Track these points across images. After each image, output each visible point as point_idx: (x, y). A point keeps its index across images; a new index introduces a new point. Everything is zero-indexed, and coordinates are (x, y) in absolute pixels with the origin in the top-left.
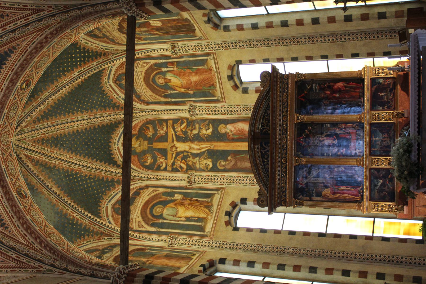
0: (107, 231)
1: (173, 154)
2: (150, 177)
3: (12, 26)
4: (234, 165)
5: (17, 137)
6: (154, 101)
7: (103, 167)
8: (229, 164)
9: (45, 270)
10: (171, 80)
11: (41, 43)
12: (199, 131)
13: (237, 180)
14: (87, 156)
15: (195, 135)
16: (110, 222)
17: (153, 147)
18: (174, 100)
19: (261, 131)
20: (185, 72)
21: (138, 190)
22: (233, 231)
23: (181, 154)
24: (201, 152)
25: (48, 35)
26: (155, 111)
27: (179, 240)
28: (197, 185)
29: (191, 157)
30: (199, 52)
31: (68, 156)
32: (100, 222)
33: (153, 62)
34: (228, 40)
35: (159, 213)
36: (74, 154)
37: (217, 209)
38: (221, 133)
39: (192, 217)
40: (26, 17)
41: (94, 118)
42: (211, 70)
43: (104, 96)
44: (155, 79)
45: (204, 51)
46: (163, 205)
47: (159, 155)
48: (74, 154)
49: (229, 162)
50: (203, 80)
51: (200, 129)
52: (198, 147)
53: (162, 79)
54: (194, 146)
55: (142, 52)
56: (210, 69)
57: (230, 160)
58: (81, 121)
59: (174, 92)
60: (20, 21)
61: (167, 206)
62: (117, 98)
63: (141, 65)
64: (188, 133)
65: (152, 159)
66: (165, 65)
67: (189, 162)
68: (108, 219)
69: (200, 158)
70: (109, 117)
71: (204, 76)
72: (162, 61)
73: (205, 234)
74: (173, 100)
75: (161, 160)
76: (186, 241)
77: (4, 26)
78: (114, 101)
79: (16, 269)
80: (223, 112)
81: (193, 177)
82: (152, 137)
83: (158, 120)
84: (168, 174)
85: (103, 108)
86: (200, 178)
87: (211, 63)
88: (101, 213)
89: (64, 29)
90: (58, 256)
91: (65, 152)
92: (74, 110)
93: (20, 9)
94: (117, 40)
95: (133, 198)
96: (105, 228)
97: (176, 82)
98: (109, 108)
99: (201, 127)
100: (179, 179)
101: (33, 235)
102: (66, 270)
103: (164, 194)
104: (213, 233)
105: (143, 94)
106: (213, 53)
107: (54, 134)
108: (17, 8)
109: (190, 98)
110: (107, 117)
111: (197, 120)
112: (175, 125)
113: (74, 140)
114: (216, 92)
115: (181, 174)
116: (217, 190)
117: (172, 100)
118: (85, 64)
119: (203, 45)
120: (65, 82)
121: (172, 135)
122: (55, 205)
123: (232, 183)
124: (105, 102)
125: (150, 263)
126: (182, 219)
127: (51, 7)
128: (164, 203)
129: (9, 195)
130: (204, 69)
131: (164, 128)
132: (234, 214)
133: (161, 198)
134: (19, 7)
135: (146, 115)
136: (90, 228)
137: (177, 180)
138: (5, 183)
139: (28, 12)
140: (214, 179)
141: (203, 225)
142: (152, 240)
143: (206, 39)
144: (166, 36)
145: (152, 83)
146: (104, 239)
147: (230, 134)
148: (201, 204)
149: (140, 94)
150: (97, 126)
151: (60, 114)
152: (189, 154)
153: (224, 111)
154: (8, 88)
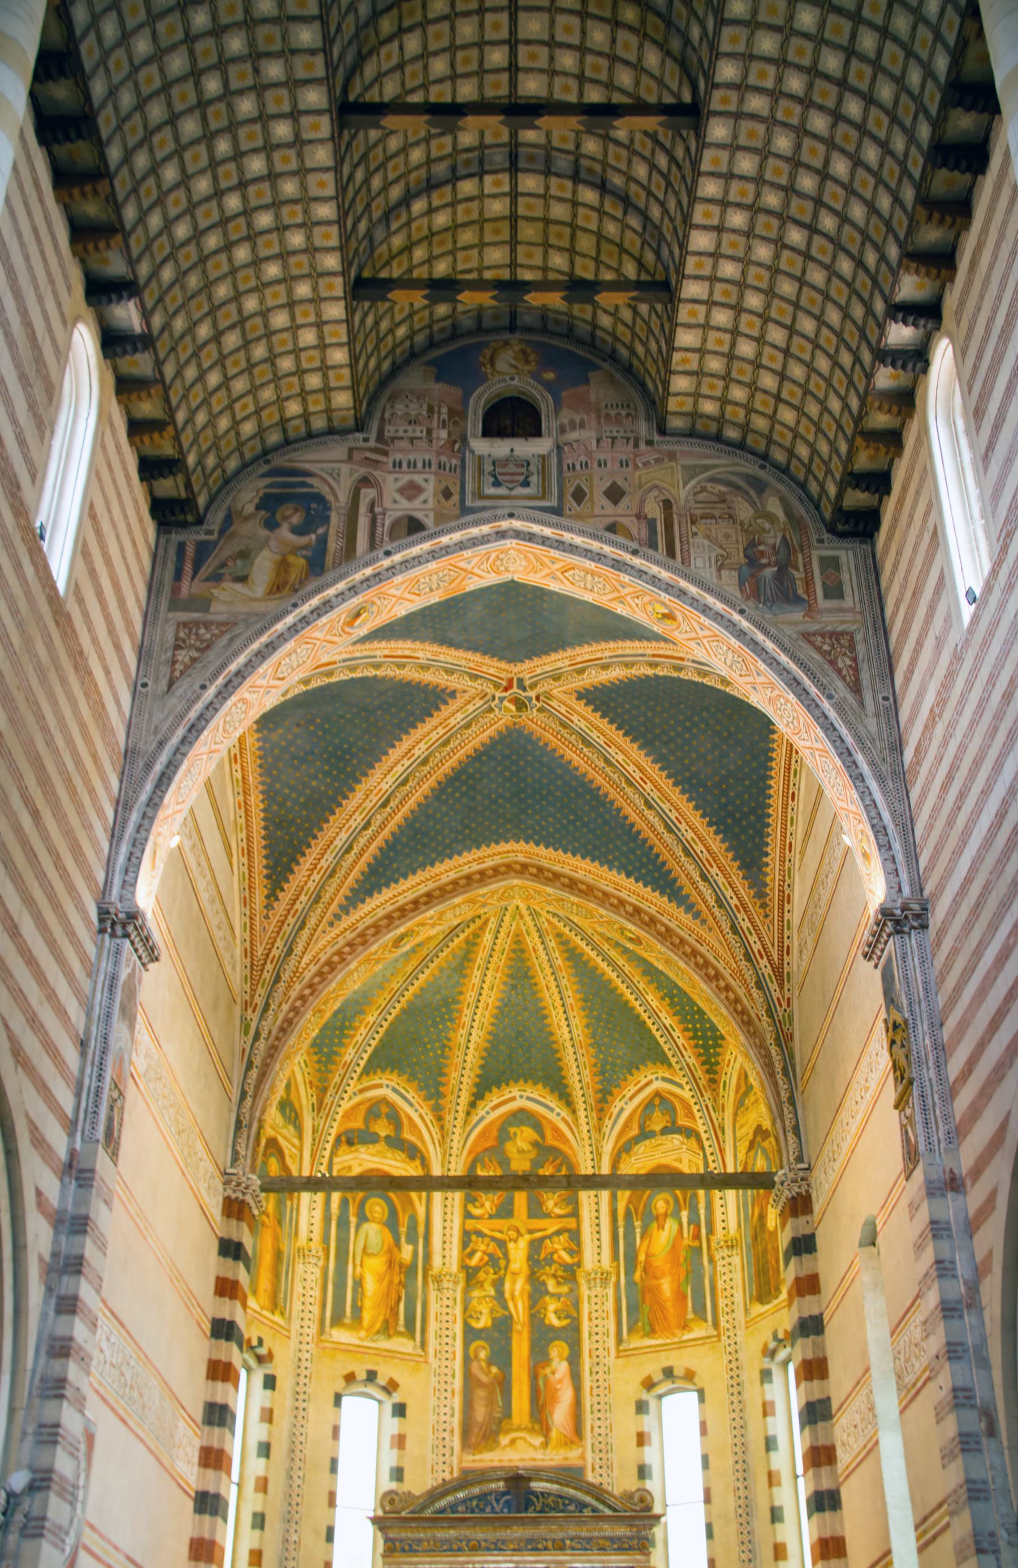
3: (746, 924)
5: (523, 907)
11: (718, 976)
12: (552, 1295)
15: (544, 1283)
20: (679, 1264)
28: (433, 1295)
30: (722, 1302)
34: (744, 1376)
50: (663, 1308)
51: (558, 1296)
52: (517, 1293)
66: (694, 1220)
70: (578, 1086)
72: (702, 1212)
74: (621, 1231)
75: (488, 1204)
78: (615, 1091)
80: (595, 1353)
86: (450, 1302)
87: (700, 1330)
90: (277, 1038)
92: (591, 1011)
98: (601, 1082)
101: (317, 979)
102: (250, 1066)
103: (413, 1219)
106: (719, 1336)
113: (525, 1009)
116: (423, 1345)
120: (650, 997)
125: (263, 1224)
126: (359, 1269)
128: (392, 1223)
132: (371, 1390)
136: (334, 1063)
144: (750, 1233)
147: (548, 1371)
151: (581, 983)
154: (622, 902)
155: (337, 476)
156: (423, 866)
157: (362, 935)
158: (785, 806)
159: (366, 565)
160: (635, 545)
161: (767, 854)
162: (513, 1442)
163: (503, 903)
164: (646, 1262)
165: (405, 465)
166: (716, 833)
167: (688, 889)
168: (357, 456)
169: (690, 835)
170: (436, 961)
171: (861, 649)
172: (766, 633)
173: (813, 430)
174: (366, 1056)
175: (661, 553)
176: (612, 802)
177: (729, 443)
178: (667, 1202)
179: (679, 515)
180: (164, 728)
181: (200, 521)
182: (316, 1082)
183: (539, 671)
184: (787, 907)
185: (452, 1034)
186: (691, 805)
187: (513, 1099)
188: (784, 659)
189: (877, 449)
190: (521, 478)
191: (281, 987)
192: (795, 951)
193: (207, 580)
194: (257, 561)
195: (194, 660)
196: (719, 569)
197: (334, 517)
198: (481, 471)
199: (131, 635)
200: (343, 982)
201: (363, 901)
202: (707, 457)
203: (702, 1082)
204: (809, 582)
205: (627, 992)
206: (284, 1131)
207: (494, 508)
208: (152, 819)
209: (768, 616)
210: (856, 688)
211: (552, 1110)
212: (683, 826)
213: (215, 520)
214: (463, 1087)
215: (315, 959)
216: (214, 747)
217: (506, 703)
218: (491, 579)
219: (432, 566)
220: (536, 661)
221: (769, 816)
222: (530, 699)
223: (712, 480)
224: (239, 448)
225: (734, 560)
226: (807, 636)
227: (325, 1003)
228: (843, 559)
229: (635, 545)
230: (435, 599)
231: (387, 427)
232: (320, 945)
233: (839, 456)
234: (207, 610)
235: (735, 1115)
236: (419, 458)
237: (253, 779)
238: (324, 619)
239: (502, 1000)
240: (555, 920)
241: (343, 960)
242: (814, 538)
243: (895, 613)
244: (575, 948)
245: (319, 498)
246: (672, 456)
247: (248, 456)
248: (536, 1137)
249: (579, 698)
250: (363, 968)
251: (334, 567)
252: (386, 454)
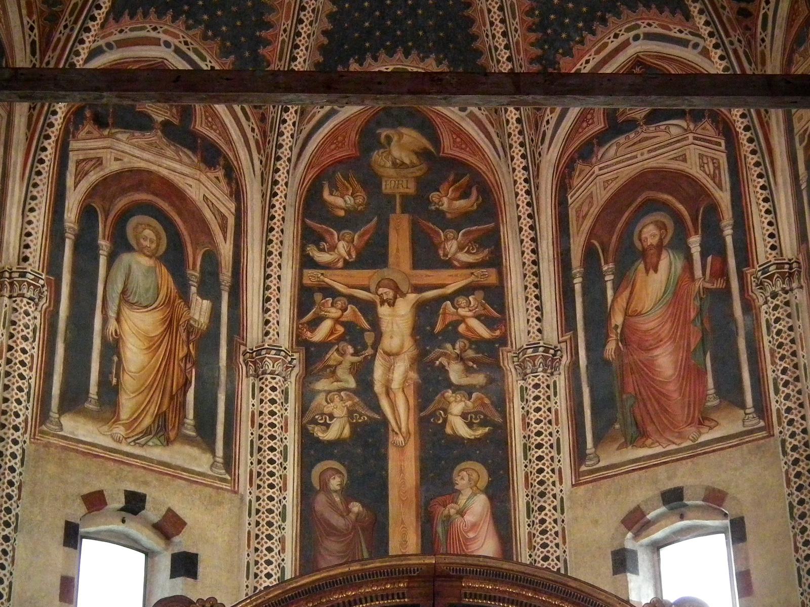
0: (63, 39)
1: (366, 289)
2: (277, 204)
4: (329, 525)
6: (572, 213)
7: (311, 24)
8: (332, 504)
10: (656, 271)
12: (457, 388)
13: (269, 537)
15: (443, 370)
17: (392, 216)
18: (578, 288)
21: (226, 158)
22: (63, 524)
23: (368, 321)
24: (375, 396)
26: (530, 216)
27: (27, 313)
28: (245, 385)
32: (96, 12)
33: (724, 198)
37: (151, 460)
38: (455, 472)
42: (700, 423)
43: (585, 22)
44: (656, 210)
45: (777, 391)
46: (166, 252)
47: (360, 237)
49: (341, 507)
50: (660, 397)
51: (468, 391)
52: (395, 385)
53: (657, 238)
54: (401, 368)
55: (759, 154)
56: (705, 418)
57: (349, 511)
59: (609, 285)
61: (164, 270)
63: (710, 153)
64: (449, 346)
65: (347, 211)
67: (337, 350)
68: (109, 46)
69: (355, 392)
70: (501, 42)
72: (728, 232)
73: (54, 415)
75: (342, 247)
76: (25, 339)
80: (535, 478)
81: (278, 369)
82: (433, 208)
83: (496, 231)
84: (288, 273)
85: (537, 20)
86: (277, 396)
88: (131, 18)
95: (195, 141)
96: (72, 29)
97: (650, 290)
99: (474, 395)
103: (211, 259)
104: (56, 447)
105: (596, 168)
106: (769, 427)
109: (588, 349)
110: (505, 34)
111: (503, 377)
112: (480, 294)
114: (616, 446)
115: (292, 320)
116: (229, 463)
117: (575, 281)
119: (799, 385)
121: (442, 286)
123: (256, 517)
124: (562, 24)
126: (112, 326)
130: (704, 396)
131: (468, 252)
132: (133, 528)
133: (196, 244)
135: (515, 182)
137: (267, 305)
140: (272, 449)
141: (87, 405)
142: (28, 207)
145: (639, 200)
146: (32, 29)
147: (452, 510)
148: (172, 398)
149: (594, 160)
152: (369, 351)
153: (541, 483)
178: (662, 226)
203: (727, 14)
248: (425, 143)
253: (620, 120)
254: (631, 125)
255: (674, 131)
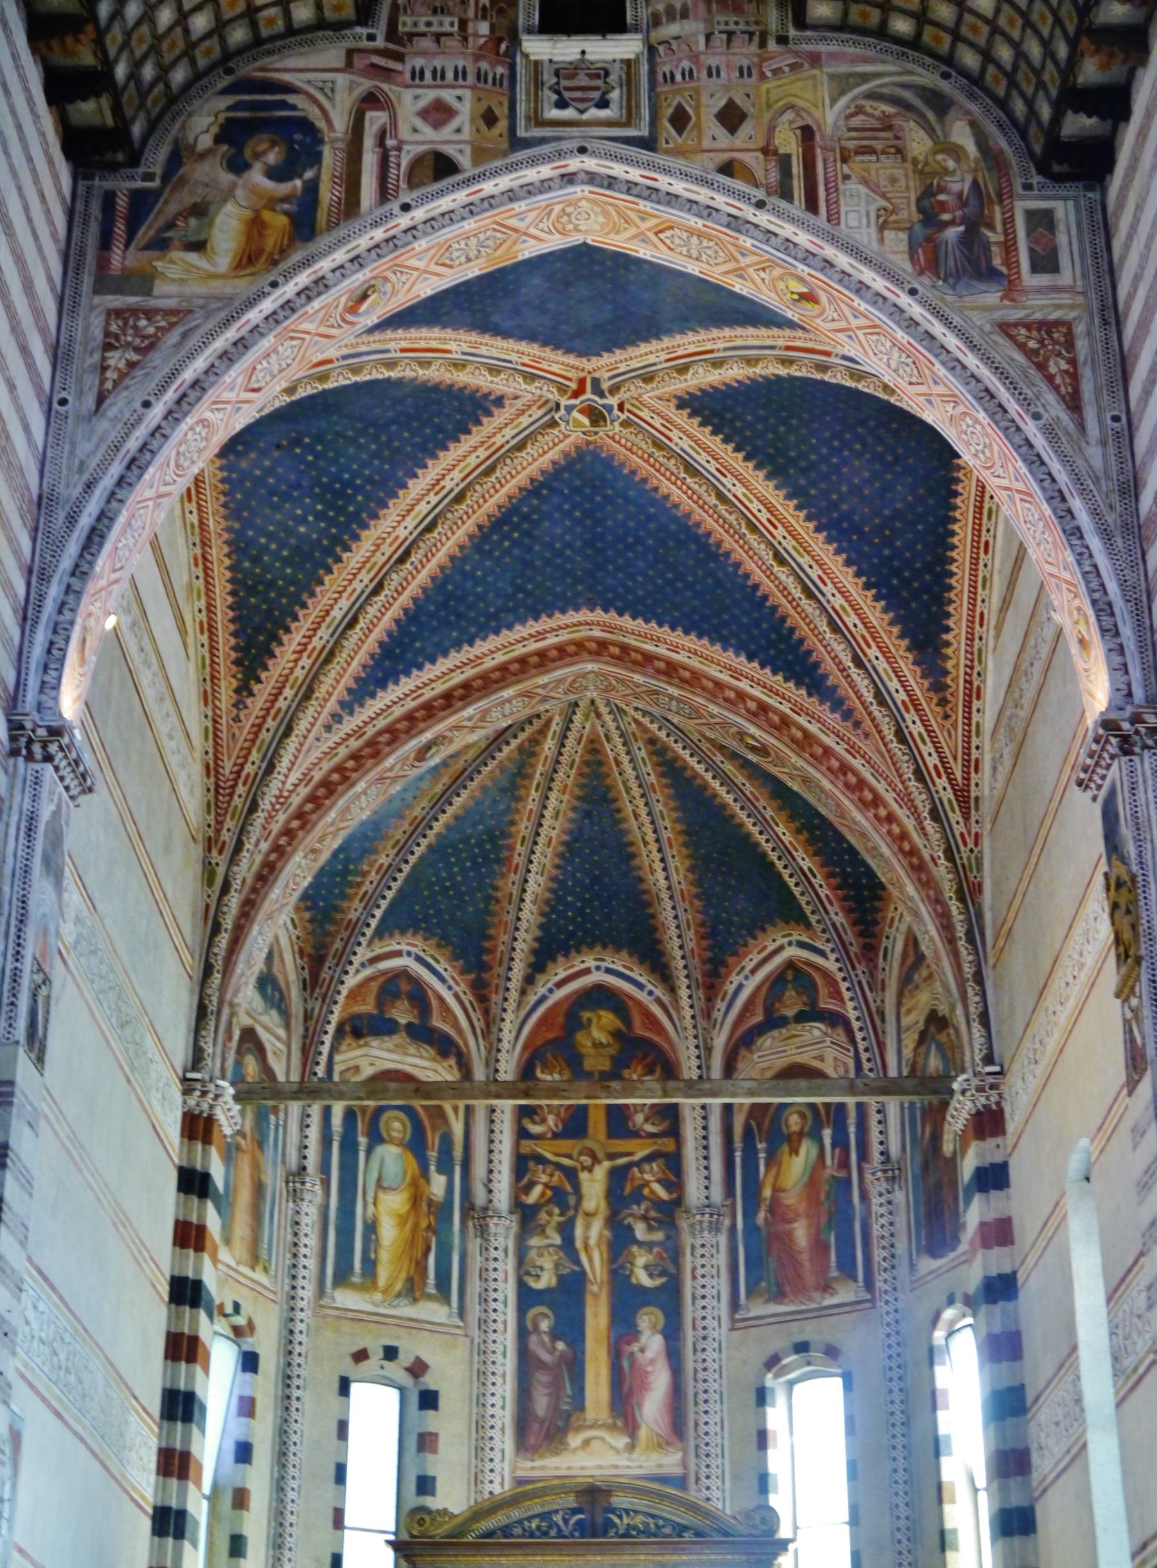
1: (569, 1157)
3: (917, 729)
4: (540, 1361)
8: (543, 1344)
9: (214, 862)
10: (797, 1153)
11: (877, 801)
12: (640, 1244)
13: (493, 1374)
14: (555, 886)
15: (630, 1229)
16: (358, 971)
18: (738, 1160)
19: (613, 1511)
20: (818, 1203)
21: (457, 1047)
22: (337, 1379)
25: (900, 824)
28: (474, 1244)
29: (561, 1219)
30: (878, 1254)
31: (554, 834)
35: (388, 1131)
36: (561, 849)
39: (377, 1240)
40: (945, 768)
41: (674, 908)
48: (561, 849)
50: (796, 1264)
51: (648, 1246)
52: (592, 1242)
57: (554, 1349)
58: (665, 869)
59: (762, 1164)
60: (932, 751)
61: (410, 1155)
62: (743, 968)
64: (635, 1207)
66: (840, 1141)
70: (678, 953)
71: (807, 1264)
72: (852, 1129)
74: (738, 1155)
77: (915, 705)
78: (731, 960)
79: (212, 779)
80: (700, 1324)
87: (846, 1293)
89: (915, 877)
91: (568, 826)
93: (967, 752)
94: (912, 996)
98: (711, 948)
99: (655, 1250)
100: (494, 1186)
105: (755, 1057)
106: (872, 1301)
107: (619, 792)
108: (969, 743)
109: (745, 1216)
110: (681, 947)
113: (604, 846)
116: (462, 1313)
118: (836, 888)
120: (780, 830)
122: (401, 817)
124: (729, 932)
125: (238, 1148)
126: (371, 1209)
127: (976, 844)
128: (416, 1145)
129: (424, 720)
130: (827, 1266)
133: (434, 1128)
134: (973, 750)
136: (334, 922)
138: (460, 704)
139: (959, 775)
143: (912, 1282)
144: (919, 1159)
147: (635, 1347)
148: (417, 1263)
150: (650, 911)
152: (571, 1213)
153: (704, 1328)
155: (329, 91)
156: (458, 645)
157: (371, 743)
158: (975, 561)
159: (375, 224)
160: (760, 194)
161: (948, 630)
162: (587, 1443)
163: (572, 697)
164: (774, 1199)
165: (428, 75)
166: (876, 598)
167: (835, 678)
168: (360, 62)
169: (838, 601)
170: (478, 779)
171: (1082, 346)
172: (948, 323)
173: (1019, 22)
174: (378, 913)
175: (797, 207)
176: (727, 555)
177: (898, 40)
179: (824, 149)
180: (93, 463)
181: (134, 159)
182: (309, 949)
183: (623, 368)
184: (976, 704)
185: (500, 883)
186: (841, 559)
187: (587, 971)
188: (972, 361)
189: (1111, 55)
190: (596, 95)
191: (260, 817)
192: (986, 766)
193: (147, 247)
194: (219, 220)
195: (132, 365)
196: (882, 228)
197: (327, 152)
198: (538, 84)
199: (43, 331)
200: (347, 809)
201: (373, 696)
202: (866, 60)
203: (854, 950)
204: (1009, 247)
205: (749, 822)
206: (265, 1019)
207: (558, 139)
208: (79, 594)
209: (949, 298)
210: (1074, 404)
211: (640, 986)
212: (829, 589)
213: (157, 158)
214: (518, 955)
215: (306, 778)
216: (163, 489)
217: (575, 414)
218: (555, 243)
219: (470, 225)
220: (619, 355)
221: (952, 574)
222: (609, 408)
223: (871, 96)
224: (189, 52)
225: (904, 215)
226: (1005, 328)
227: (321, 840)
228: (1060, 214)
229: (760, 194)
230: (473, 271)
231: (402, 19)
232: (312, 758)
233: (1056, 63)
234: (148, 292)
235: (900, 995)
236: (449, 63)
237: (214, 525)
238: (316, 304)
239: (570, 832)
240: (646, 721)
241: (345, 779)
242: (1018, 183)
243: (1131, 296)
244: (677, 758)
245: (306, 125)
246: (815, 60)
247: (202, 62)
248: (619, 1024)
249: (680, 407)
250: (373, 791)
251: (331, 227)
252: (400, 58)
253: (776, 1015)
254: (783, 1022)
255: (816, 1033)
